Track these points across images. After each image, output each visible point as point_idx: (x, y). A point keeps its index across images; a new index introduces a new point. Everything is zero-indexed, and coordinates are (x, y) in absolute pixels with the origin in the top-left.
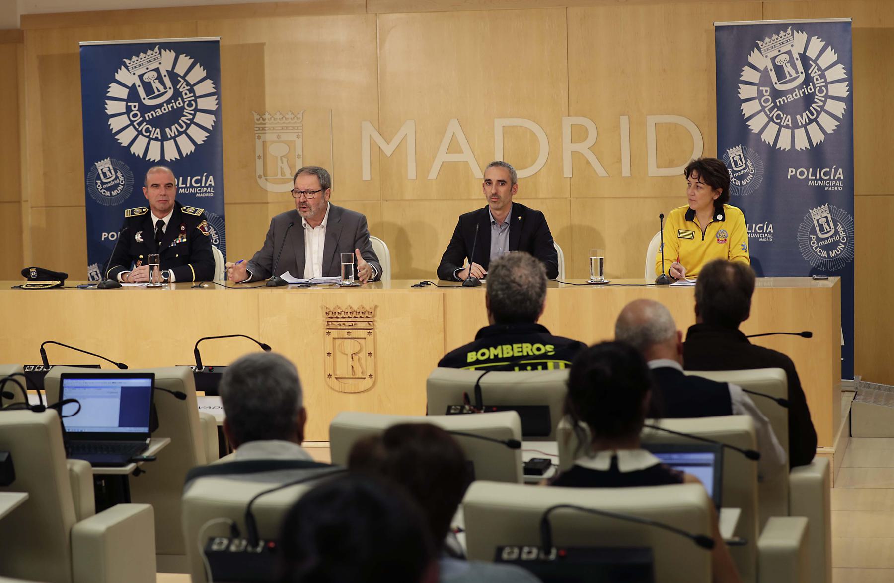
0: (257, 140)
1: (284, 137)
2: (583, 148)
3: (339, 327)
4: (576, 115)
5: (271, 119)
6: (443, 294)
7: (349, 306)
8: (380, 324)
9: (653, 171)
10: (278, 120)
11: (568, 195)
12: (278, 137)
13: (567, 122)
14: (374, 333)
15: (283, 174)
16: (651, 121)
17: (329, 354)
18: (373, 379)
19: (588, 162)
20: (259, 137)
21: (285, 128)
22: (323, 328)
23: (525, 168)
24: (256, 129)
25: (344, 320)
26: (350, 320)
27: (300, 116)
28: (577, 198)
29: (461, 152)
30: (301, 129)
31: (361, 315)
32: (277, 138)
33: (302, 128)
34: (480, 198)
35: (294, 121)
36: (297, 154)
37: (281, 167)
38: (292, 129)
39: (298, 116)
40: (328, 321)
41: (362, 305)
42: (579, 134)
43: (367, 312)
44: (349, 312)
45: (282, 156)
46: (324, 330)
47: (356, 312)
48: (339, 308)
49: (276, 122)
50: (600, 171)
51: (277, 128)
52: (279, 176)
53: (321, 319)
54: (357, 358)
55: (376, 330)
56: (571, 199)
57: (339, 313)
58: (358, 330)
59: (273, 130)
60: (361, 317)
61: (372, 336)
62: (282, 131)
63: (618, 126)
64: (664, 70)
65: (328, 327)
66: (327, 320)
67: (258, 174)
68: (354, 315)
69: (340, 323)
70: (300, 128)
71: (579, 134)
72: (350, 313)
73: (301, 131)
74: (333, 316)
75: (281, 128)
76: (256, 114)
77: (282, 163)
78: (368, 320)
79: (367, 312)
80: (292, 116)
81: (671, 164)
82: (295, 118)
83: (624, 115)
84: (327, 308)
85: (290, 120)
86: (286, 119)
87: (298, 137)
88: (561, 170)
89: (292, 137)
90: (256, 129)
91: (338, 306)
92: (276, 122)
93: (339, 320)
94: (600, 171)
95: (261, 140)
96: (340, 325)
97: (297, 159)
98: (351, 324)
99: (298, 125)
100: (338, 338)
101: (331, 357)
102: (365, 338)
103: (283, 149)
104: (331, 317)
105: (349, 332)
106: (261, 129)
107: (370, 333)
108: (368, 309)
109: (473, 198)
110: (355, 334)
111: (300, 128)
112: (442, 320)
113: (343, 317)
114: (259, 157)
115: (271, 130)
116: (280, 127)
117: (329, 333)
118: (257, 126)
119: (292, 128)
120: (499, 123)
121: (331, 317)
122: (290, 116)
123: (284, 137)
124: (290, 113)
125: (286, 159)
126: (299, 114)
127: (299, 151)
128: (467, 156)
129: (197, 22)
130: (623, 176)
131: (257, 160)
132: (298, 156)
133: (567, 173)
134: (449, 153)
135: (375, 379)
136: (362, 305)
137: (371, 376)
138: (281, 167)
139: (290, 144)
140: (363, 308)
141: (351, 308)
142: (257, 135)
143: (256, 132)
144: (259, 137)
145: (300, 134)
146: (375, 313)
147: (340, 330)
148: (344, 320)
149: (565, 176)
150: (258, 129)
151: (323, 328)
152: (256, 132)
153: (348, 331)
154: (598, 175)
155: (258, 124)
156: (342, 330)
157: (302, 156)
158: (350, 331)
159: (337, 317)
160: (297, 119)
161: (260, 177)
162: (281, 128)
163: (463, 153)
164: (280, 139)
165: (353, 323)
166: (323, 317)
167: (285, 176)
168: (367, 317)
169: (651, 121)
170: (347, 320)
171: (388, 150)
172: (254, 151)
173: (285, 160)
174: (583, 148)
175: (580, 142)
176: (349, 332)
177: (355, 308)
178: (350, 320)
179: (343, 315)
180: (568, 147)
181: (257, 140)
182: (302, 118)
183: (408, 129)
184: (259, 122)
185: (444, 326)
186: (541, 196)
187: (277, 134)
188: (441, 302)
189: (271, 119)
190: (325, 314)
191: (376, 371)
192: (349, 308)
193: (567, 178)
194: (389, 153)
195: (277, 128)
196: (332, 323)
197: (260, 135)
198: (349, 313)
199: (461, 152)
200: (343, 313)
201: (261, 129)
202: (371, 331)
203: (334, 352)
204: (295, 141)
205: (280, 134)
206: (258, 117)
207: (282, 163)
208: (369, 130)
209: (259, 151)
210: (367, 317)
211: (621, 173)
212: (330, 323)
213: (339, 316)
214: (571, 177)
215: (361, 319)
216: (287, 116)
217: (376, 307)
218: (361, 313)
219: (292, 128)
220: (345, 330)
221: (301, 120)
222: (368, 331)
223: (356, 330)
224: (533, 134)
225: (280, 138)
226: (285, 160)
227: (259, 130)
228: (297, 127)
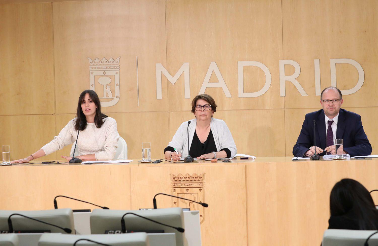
0: (91, 75)
1: (108, 73)
2: (292, 78)
3: (181, 187)
5: (99, 62)
6: (245, 165)
7: (188, 173)
8: (207, 185)
10: (104, 63)
11: (283, 107)
12: (104, 73)
13: (282, 63)
14: (203, 189)
15: (107, 96)
16: (333, 62)
17: (175, 203)
18: (202, 218)
19: (295, 87)
20: (92, 73)
21: (109, 68)
22: (171, 187)
23: (257, 91)
24: (90, 68)
25: (184, 182)
26: (188, 182)
27: (118, 60)
28: (288, 109)
29: (217, 81)
31: (195, 179)
33: (119, 68)
34: (229, 109)
35: (114, 63)
36: (116, 83)
39: (117, 60)
40: (174, 183)
41: (195, 173)
42: (289, 70)
43: (198, 177)
44: (187, 178)
45: (107, 85)
46: (172, 188)
47: (192, 177)
48: (181, 175)
49: (103, 64)
50: (303, 93)
51: (103, 68)
52: (105, 97)
53: (170, 182)
54: (193, 205)
55: (204, 188)
56: (285, 109)
57: (181, 178)
58: (193, 188)
60: (195, 180)
61: (202, 191)
62: (106, 70)
63: (313, 65)
64: (341, 32)
65: (174, 187)
66: (174, 182)
68: (191, 179)
69: (182, 184)
70: (117, 68)
71: (289, 70)
72: (188, 178)
74: (177, 180)
76: (90, 59)
77: (107, 89)
78: (199, 182)
79: (198, 177)
80: (113, 60)
82: (115, 62)
84: (173, 175)
85: (111, 63)
86: (109, 62)
87: (117, 73)
88: (279, 91)
89: (112, 73)
90: (90, 68)
91: (180, 174)
92: (103, 64)
93: (181, 182)
94: (303, 93)
95: (93, 75)
96: (182, 185)
98: (188, 184)
99: (117, 66)
100: (180, 193)
101: (176, 205)
102: (197, 193)
103: (108, 81)
104: (176, 181)
105: (188, 190)
106: (93, 68)
107: (200, 190)
108: (199, 175)
109: (225, 109)
110: (191, 190)
111: (117, 68)
112: (245, 181)
113: (184, 181)
115: (100, 69)
117: (175, 190)
118: (90, 66)
119: (112, 68)
120: (241, 65)
121: (176, 181)
122: (111, 60)
123: (108, 73)
124: (111, 59)
127: (117, 81)
128: (221, 84)
129: (52, 3)
130: (316, 95)
132: (117, 85)
133: (283, 94)
134: (211, 82)
135: (204, 217)
136: (195, 173)
137: (201, 215)
139: (112, 78)
140: (196, 175)
141: (188, 175)
142: (91, 72)
143: (90, 70)
145: (118, 71)
146: (203, 178)
147: (182, 188)
148: (184, 182)
150: (91, 68)
151: (171, 187)
152: (90, 70)
153: (187, 189)
155: (92, 65)
156: (183, 188)
157: (119, 85)
158: (188, 189)
159: (180, 181)
160: (116, 62)
163: (219, 82)
165: (191, 184)
166: (171, 181)
167: (109, 97)
168: (199, 180)
169: (333, 62)
170: (186, 182)
171: (173, 80)
172: (89, 82)
173: (108, 87)
174: (292, 78)
175: (289, 75)
176: (188, 190)
177: (191, 175)
178: (188, 182)
179: (184, 179)
180: (283, 78)
181: (91, 75)
183: (185, 68)
184: (92, 64)
185: (246, 185)
186: (267, 108)
187: (104, 71)
188: (244, 171)
189: (99, 62)
190: (173, 178)
191: (204, 213)
192: (187, 175)
194: (173, 83)
195: (103, 68)
196: (177, 185)
197: (93, 72)
198: (187, 178)
199: (217, 81)
200: (184, 178)
201: (93, 68)
202: (201, 188)
203: (178, 202)
205: (105, 71)
206: (92, 61)
207: (107, 89)
208: (160, 69)
209: (92, 82)
210: (199, 180)
211: (315, 94)
212: (176, 184)
213: (181, 180)
215: (195, 182)
216: (109, 61)
217: (204, 174)
218: (195, 178)
219: (112, 68)
220: (185, 188)
222: (199, 188)
223: (192, 188)
224: (261, 71)
226: (108, 87)
227: (92, 69)
228: (116, 67)
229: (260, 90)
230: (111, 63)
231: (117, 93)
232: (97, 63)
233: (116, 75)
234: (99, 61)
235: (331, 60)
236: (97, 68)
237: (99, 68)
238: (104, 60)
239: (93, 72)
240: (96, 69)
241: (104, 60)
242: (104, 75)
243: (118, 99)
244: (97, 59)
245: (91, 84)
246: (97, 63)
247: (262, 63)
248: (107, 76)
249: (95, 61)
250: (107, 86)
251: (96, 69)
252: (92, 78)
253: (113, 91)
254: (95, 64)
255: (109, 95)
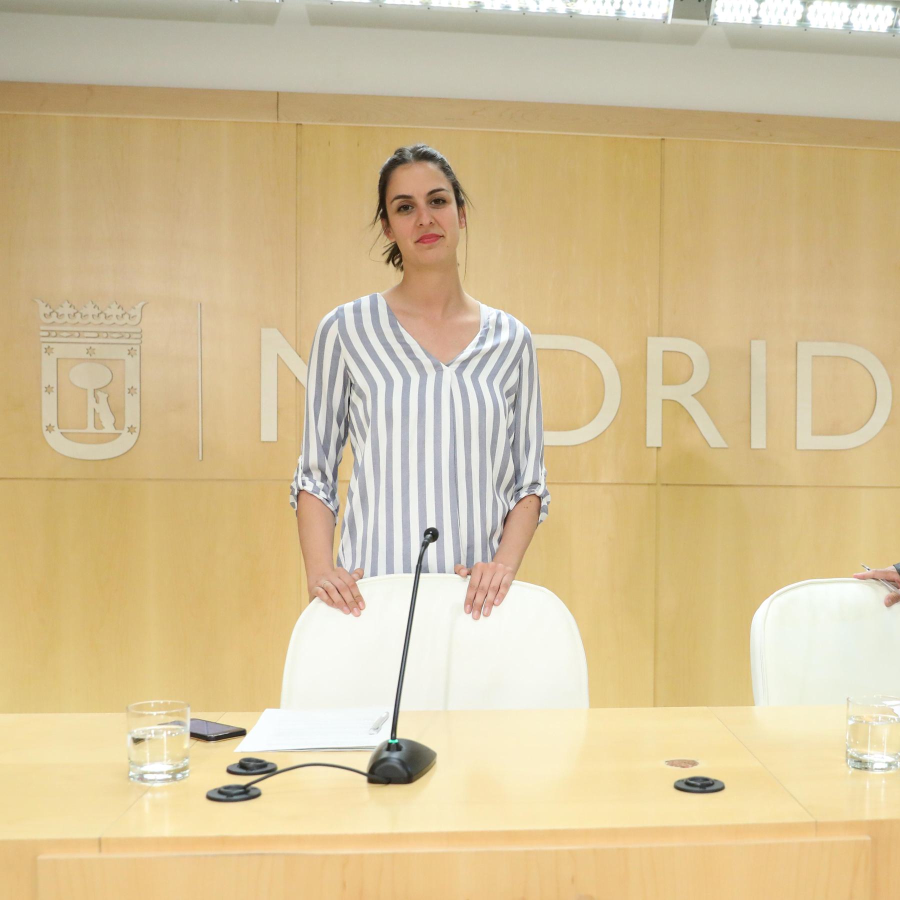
0: (45, 356)
4: (671, 336)
9: (806, 440)
10: (90, 319)
13: (656, 347)
15: (98, 424)
16: (807, 350)
20: (48, 351)
23: (577, 427)
27: (136, 312)
30: (136, 339)
32: (87, 353)
33: (138, 336)
36: (128, 386)
37: (95, 410)
38: (118, 338)
39: (132, 313)
45: (97, 389)
49: (86, 322)
51: (86, 335)
52: (91, 429)
59: (79, 337)
67: (45, 424)
73: (138, 341)
75: (95, 335)
77: (97, 402)
80: (120, 312)
81: (835, 430)
83: (756, 339)
97: (128, 396)
114: (48, 389)
116: (95, 332)
118: (42, 328)
122: (114, 311)
124: (114, 306)
125: (107, 395)
126: (134, 308)
127: (132, 381)
131: (45, 395)
132: (131, 391)
133: (654, 438)
138: (95, 410)
142: (46, 345)
144: (48, 351)
145: (135, 347)
149: (648, 445)
150: (46, 334)
154: (710, 446)
157: (138, 391)
161: (50, 428)
162: (95, 335)
164: (93, 356)
167: (103, 428)
169: (807, 350)
172: (39, 378)
173: (102, 396)
174: (683, 394)
181: (45, 356)
182: (139, 315)
184: (50, 321)
187: (88, 346)
193: (652, 447)
195: (86, 335)
197: (51, 345)
201: (54, 334)
204: (124, 360)
205: (93, 346)
206: (48, 311)
209: (49, 378)
214: (659, 445)
216: (108, 312)
221: (137, 319)
225: (94, 353)
226: (102, 396)
227: (49, 336)
229: (584, 425)
230: (114, 319)
231: (131, 417)
232: (66, 318)
233: (128, 359)
234: (72, 311)
235: (798, 343)
236: (65, 334)
237: (71, 334)
238: (90, 310)
239: (51, 345)
240: (63, 337)
241: (90, 310)
242: (88, 356)
243: (135, 435)
244: (66, 305)
245: (45, 384)
246: (66, 318)
247: (595, 342)
248: (102, 361)
249: (60, 311)
250: (99, 393)
251: (63, 337)
252: (48, 365)
253: (117, 413)
254: (59, 321)
255: (104, 424)
